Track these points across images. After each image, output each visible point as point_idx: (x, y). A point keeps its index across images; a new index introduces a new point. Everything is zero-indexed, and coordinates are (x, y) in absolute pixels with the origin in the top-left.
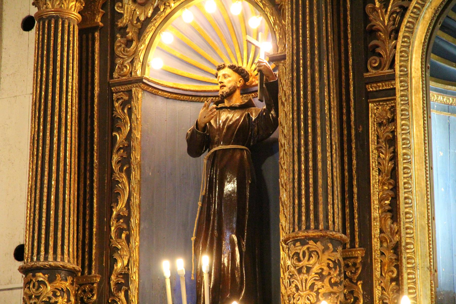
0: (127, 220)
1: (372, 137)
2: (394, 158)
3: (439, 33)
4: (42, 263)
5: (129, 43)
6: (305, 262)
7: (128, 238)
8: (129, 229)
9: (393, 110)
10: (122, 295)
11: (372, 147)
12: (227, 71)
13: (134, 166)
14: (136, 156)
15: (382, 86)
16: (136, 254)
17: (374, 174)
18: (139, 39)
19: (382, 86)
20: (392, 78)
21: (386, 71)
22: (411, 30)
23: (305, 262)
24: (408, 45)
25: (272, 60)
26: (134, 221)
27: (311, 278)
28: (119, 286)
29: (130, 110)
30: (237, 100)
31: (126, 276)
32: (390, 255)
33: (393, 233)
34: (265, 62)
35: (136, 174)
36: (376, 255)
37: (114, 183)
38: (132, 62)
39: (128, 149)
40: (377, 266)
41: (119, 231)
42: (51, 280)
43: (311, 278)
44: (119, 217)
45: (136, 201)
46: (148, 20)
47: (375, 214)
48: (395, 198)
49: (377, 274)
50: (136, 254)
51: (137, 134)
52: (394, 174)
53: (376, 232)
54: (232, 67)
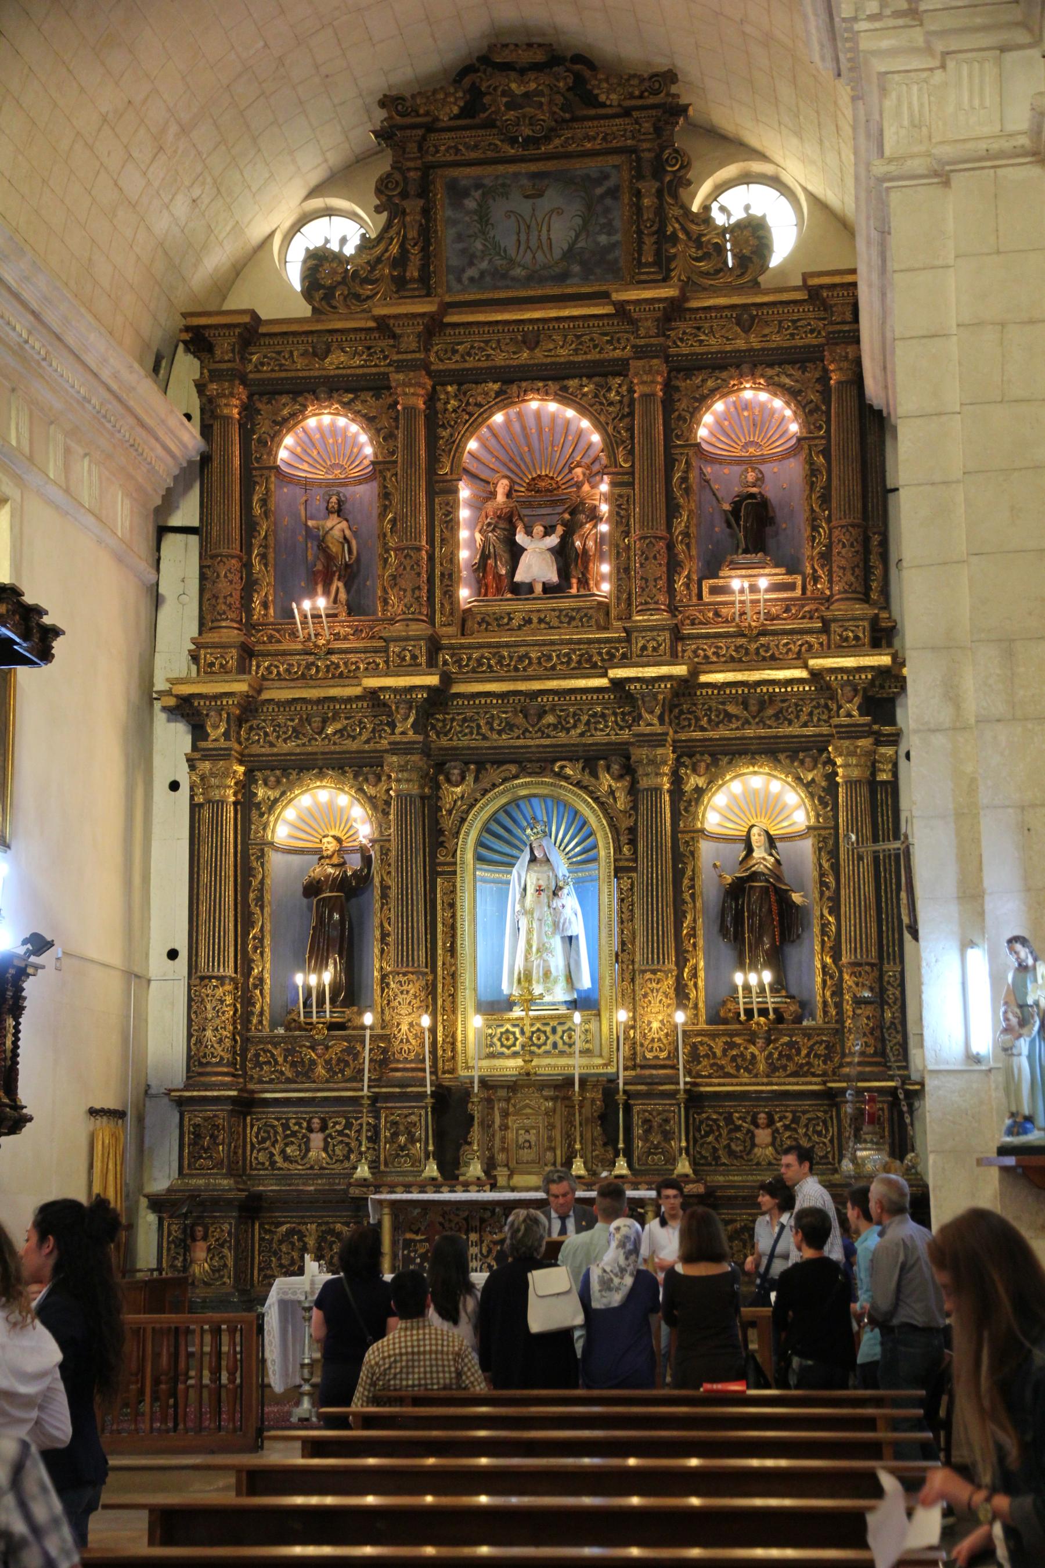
0: (261, 940)
1: (439, 901)
2: (454, 916)
3: (484, 834)
4: (216, 974)
5: (262, 815)
6: (405, 988)
7: (262, 954)
8: (262, 946)
9: (454, 886)
10: (258, 992)
11: (439, 907)
12: (330, 839)
13: (266, 903)
14: (267, 897)
15: (447, 869)
16: (268, 965)
17: (440, 926)
18: (270, 814)
19: (447, 869)
20: (455, 864)
21: (449, 859)
22: (467, 834)
23: (405, 988)
24: (465, 843)
25: (371, 841)
26: (267, 942)
27: (409, 997)
28: (255, 987)
29: (262, 864)
30: (335, 860)
31: (261, 980)
32: (449, 979)
33: (451, 965)
34: (365, 841)
35: (267, 910)
36: (440, 978)
37: (251, 914)
38: (264, 829)
39: (261, 890)
40: (440, 986)
41: (255, 948)
42: (222, 985)
43: (409, 997)
44: (254, 938)
45: (268, 927)
46: (276, 801)
47: (440, 951)
48: (453, 944)
49: (440, 990)
50: (268, 965)
51: (268, 881)
52: (453, 927)
53: (440, 963)
54: (334, 837)
